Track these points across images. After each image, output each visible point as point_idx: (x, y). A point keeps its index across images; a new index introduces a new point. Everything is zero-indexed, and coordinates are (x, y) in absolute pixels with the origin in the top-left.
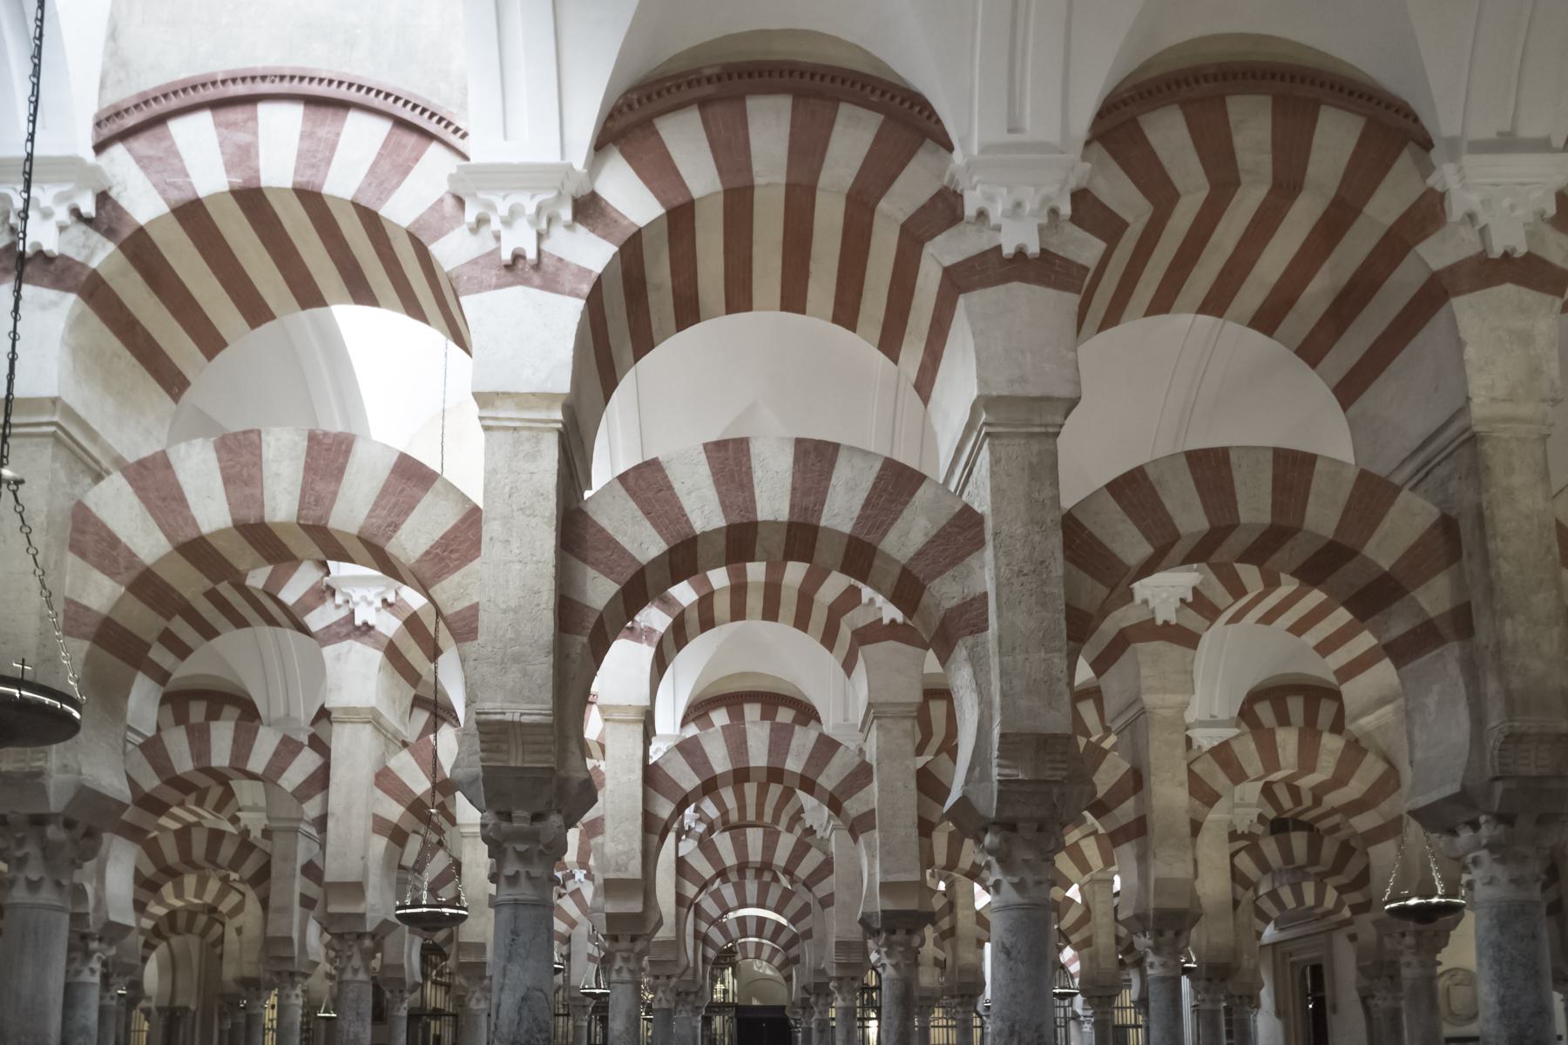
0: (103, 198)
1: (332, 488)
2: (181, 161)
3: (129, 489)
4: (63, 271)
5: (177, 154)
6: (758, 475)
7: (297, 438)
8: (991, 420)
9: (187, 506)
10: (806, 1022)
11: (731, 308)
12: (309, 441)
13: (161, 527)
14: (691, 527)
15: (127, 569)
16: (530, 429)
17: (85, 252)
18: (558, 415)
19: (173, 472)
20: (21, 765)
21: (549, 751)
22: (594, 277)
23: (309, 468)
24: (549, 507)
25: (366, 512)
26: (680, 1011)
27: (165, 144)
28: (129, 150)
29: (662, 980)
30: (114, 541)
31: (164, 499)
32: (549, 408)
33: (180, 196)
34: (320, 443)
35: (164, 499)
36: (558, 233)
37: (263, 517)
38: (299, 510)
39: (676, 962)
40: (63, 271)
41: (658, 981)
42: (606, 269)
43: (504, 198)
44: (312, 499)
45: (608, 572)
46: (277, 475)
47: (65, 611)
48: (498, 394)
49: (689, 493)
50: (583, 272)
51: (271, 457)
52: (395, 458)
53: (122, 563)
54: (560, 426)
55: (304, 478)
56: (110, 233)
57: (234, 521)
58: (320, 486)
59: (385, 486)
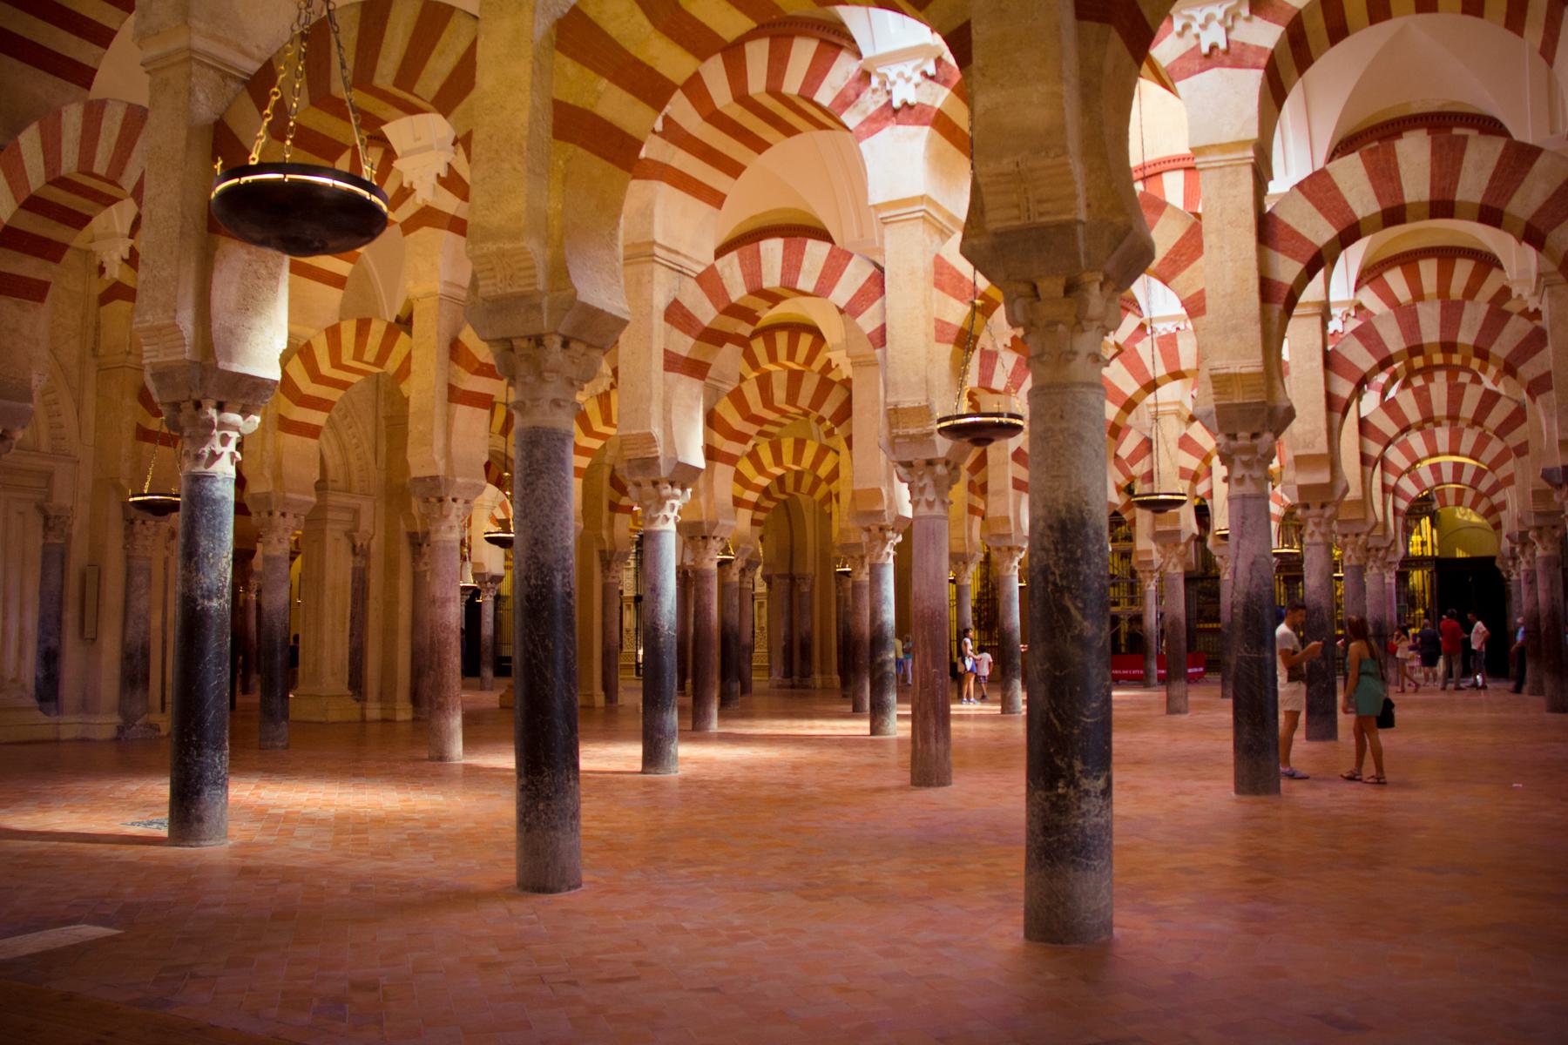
11: (1373, 21)
14: (1354, 216)
16: (1231, 166)
18: (1251, 153)
20: (920, 429)
22: (1269, 53)
24: (1250, 219)
26: (1371, 568)
29: (1350, 539)
32: (1244, 149)
36: (1240, 25)
39: (1364, 521)
41: (1347, 540)
42: (1277, 45)
43: (1201, 11)
45: (1294, 255)
49: (1351, 190)
50: (1260, 50)
54: (1252, 160)
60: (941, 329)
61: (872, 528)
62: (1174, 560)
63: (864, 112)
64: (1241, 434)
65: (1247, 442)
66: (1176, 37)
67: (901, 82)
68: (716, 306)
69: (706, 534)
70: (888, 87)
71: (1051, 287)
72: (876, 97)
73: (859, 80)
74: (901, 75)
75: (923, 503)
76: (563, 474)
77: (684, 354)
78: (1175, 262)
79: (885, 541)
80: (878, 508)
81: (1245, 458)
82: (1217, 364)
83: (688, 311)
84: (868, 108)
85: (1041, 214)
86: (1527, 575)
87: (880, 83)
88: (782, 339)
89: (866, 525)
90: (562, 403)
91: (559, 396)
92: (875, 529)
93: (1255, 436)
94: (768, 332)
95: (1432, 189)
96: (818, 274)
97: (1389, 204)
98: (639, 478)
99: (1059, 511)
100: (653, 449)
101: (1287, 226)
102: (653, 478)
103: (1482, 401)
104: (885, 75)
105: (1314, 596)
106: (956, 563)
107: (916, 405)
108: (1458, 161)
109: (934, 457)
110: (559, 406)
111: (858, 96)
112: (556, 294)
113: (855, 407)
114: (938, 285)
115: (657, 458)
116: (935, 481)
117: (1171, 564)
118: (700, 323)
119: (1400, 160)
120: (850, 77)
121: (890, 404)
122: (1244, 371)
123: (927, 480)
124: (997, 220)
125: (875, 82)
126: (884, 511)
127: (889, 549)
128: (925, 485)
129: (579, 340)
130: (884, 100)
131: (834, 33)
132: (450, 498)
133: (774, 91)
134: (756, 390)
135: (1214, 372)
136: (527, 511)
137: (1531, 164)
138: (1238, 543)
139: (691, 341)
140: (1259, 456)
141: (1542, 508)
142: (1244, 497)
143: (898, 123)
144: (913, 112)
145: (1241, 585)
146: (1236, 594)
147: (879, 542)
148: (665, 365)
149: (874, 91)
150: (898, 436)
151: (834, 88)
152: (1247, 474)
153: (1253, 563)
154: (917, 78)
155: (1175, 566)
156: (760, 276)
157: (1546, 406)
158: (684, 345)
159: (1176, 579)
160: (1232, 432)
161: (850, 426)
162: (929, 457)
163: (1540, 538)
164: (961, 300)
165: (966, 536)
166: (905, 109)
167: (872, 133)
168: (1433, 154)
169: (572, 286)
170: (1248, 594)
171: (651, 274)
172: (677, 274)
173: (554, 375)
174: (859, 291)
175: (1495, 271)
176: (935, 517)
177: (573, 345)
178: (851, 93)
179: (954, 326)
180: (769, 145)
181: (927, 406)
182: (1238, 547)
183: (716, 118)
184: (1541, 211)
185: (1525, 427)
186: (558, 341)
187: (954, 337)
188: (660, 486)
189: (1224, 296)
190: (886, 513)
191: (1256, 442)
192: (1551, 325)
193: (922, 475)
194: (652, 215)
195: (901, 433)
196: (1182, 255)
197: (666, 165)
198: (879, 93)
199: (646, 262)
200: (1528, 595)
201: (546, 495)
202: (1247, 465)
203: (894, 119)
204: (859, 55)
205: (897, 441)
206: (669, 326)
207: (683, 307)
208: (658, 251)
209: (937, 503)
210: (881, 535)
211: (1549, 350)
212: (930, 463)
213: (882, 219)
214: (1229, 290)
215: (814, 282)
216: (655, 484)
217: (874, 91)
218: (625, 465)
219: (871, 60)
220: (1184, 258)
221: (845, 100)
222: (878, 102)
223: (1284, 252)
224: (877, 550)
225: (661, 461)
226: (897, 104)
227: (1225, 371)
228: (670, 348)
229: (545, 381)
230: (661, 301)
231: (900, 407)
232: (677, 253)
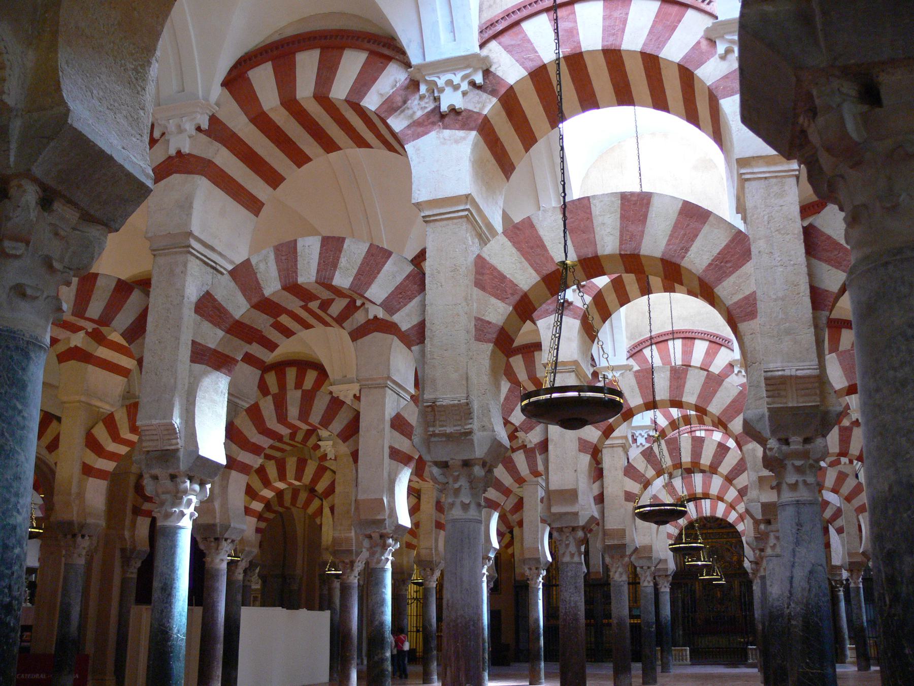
1: (640, 229)
3: (509, 244)
7: (613, 199)
9: (547, 250)
12: (621, 200)
13: (532, 266)
15: (512, 294)
21: (816, 394)
23: (623, 217)
25: (664, 242)
30: (502, 278)
31: (532, 248)
34: (629, 201)
35: (532, 248)
37: (596, 252)
38: (620, 245)
44: (628, 237)
46: (604, 224)
47: (475, 325)
48: (753, 157)
51: (597, 213)
52: (680, 205)
53: (510, 291)
55: (621, 224)
57: (578, 256)
58: (632, 228)
59: (675, 223)
60: (481, 328)
63: (411, 116)
64: (793, 439)
65: (799, 447)
66: (719, 59)
67: (448, 90)
68: (248, 299)
69: (218, 536)
70: (436, 95)
72: (423, 104)
73: (407, 88)
76: (20, 407)
77: (212, 346)
78: (721, 267)
79: (385, 547)
81: (798, 463)
82: (772, 366)
83: (220, 304)
84: (414, 113)
87: (427, 90)
88: (291, 374)
89: (368, 532)
90: (29, 292)
92: (376, 536)
93: (807, 441)
94: (279, 367)
98: (156, 471)
100: (174, 441)
101: (829, 237)
102: (171, 471)
104: (435, 83)
105: (777, 604)
106: (424, 570)
107: (456, 402)
110: (23, 295)
111: (405, 102)
113: (363, 424)
114: (479, 284)
115: (177, 450)
116: (471, 482)
118: (232, 316)
120: (398, 85)
121: (427, 402)
122: (799, 373)
123: (463, 482)
125: (423, 89)
126: (385, 520)
128: (461, 486)
129: (70, 202)
130: (431, 106)
131: (384, 46)
133: (322, 98)
134: (272, 407)
135: (769, 374)
138: (794, 551)
139: (220, 333)
140: (811, 461)
142: (798, 503)
143: (445, 128)
144: (460, 118)
145: (798, 594)
146: (793, 605)
147: (379, 549)
148: (191, 357)
150: (434, 435)
151: (381, 95)
152: (800, 479)
153: (811, 572)
154: (465, 86)
155: (621, 574)
156: (296, 273)
158: (213, 337)
160: (783, 437)
162: (465, 458)
164: (502, 299)
165: (434, 546)
166: (452, 116)
167: (419, 136)
169: (63, 103)
170: (807, 604)
171: (185, 265)
172: (212, 270)
173: (22, 245)
174: (397, 288)
176: (470, 521)
177: (57, 206)
178: (399, 99)
179: (494, 325)
180: (309, 160)
181: (468, 404)
182: (794, 556)
183: (262, 121)
187: (495, 336)
188: (178, 480)
189: (775, 300)
190: (387, 522)
191: (808, 446)
193: (458, 476)
194: (191, 207)
195: (437, 432)
196: (727, 262)
197: (209, 161)
198: (426, 100)
199: (181, 253)
202: (799, 470)
203: (441, 124)
204: (407, 65)
205: (433, 439)
206: (199, 318)
207: (215, 300)
208: (194, 243)
209: (473, 506)
212: (467, 464)
213: (423, 217)
214: (780, 294)
215: (351, 279)
216: (173, 477)
217: (422, 98)
219: (420, 68)
220: (729, 265)
221: (392, 106)
222: (425, 108)
223: (828, 261)
224: (377, 555)
225: (181, 454)
226: (444, 108)
227: (780, 373)
228: (198, 340)
230: (192, 292)
231: (438, 404)
232: (212, 249)
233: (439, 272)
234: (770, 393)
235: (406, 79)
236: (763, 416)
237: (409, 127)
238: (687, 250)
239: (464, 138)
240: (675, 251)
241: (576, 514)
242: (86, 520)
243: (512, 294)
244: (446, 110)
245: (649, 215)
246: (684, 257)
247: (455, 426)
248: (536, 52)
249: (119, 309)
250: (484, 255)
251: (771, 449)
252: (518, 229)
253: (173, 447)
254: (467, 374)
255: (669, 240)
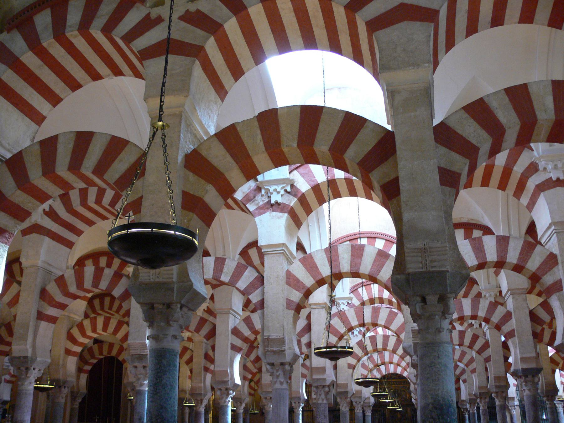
0: (292, 186)
1: (359, 261)
2: (313, 173)
3: (302, 265)
4: (283, 207)
5: (311, 172)
6: (486, 247)
8: (556, 228)
9: (318, 269)
10: (472, 410)
13: (311, 276)
15: (303, 289)
17: (289, 201)
19: (313, 259)
23: (352, 255)
27: (307, 169)
28: (298, 172)
33: (313, 184)
34: (354, 248)
40: (283, 207)
44: (354, 265)
46: (343, 258)
49: (466, 254)
51: (341, 253)
52: (377, 251)
53: (301, 287)
56: (295, 196)
60: (289, 303)
61: (222, 388)
62: (345, 405)
63: (258, 204)
67: (275, 193)
71: (432, 299)
72: (263, 198)
73: (255, 190)
74: (275, 190)
75: (278, 382)
79: (228, 394)
80: (225, 380)
85: (432, 267)
86: (483, 411)
87: (265, 192)
89: (220, 387)
90: (178, 337)
91: (175, 333)
92: (223, 389)
95: (497, 256)
96: (231, 274)
97: (481, 262)
99: (439, 401)
102: (144, 364)
103: (472, 338)
106: (237, 403)
107: (278, 337)
108: (507, 246)
109: (285, 361)
111: (254, 197)
112: (181, 284)
113: (217, 332)
114: (288, 283)
116: (284, 372)
117: (344, 407)
119: (484, 244)
120: (251, 188)
123: (280, 372)
124: (413, 267)
125: (263, 192)
127: (301, 409)
128: (279, 374)
129: (187, 307)
130: (267, 200)
132: (32, 368)
135: (413, 328)
136: (157, 391)
137: (534, 249)
141: (498, 384)
143: (273, 211)
144: (280, 207)
149: (262, 196)
150: (268, 351)
154: (282, 192)
155: (346, 407)
157: (514, 343)
159: (346, 413)
161: (214, 341)
163: (497, 397)
164: (298, 291)
165: (242, 390)
167: (261, 214)
168: (497, 243)
173: (175, 323)
175: (475, 285)
176: (284, 389)
178: (252, 195)
184: (539, 268)
185: (490, 349)
186: (179, 306)
187: (295, 307)
190: (229, 382)
192: (514, 310)
193: (278, 369)
195: (269, 350)
198: (264, 197)
200: (484, 420)
201: (168, 383)
203: (271, 209)
205: (267, 353)
209: (285, 383)
210: (226, 392)
211: (513, 320)
212: (282, 364)
217: (262, 196)
218: (130, 357)
221: (248, 198)
222: (264, 200)
224: (224, 399)
226: (273, 202)
229: (170, 325)
231: (270, 338)
233: (270, 278)
234: (414, 336)
235: (255, 186)
236: (411, 345)
237: (256, 209)
238: (380, 272)
239: (281, 217)
240: (375, 271)
241: (325, 379)
242: (67, 379)
243: (303, 289)
244: (274, 203)
245: (364, 255)
246: (378, 275)
247: (278, 347)
248: (315, 177)
249: (116, 285)
250: (290, 270)
251: (414, 360)
252: (305, 258)
253: (144, 353)
254: (283, 324)
255: (372, 267)
